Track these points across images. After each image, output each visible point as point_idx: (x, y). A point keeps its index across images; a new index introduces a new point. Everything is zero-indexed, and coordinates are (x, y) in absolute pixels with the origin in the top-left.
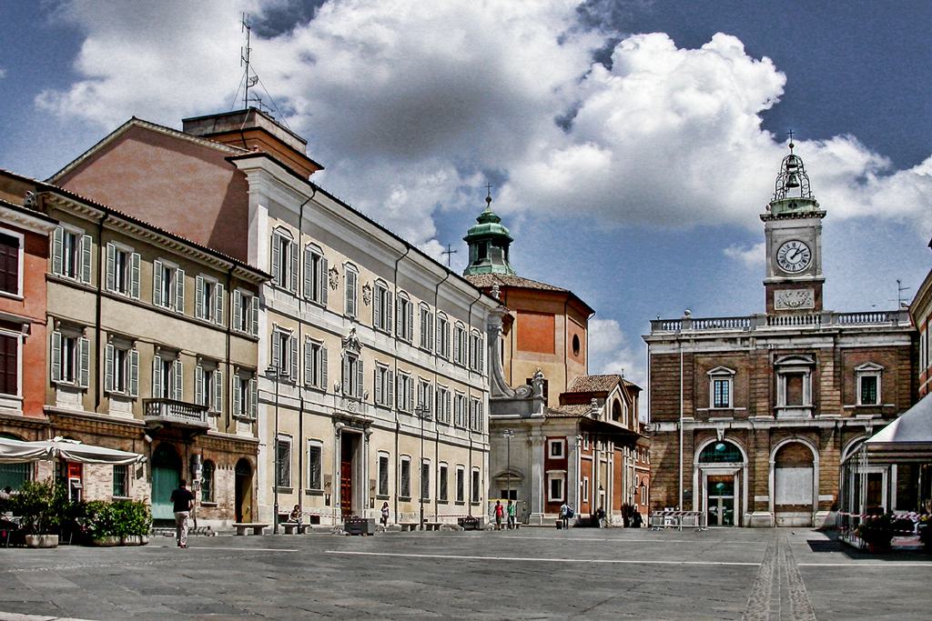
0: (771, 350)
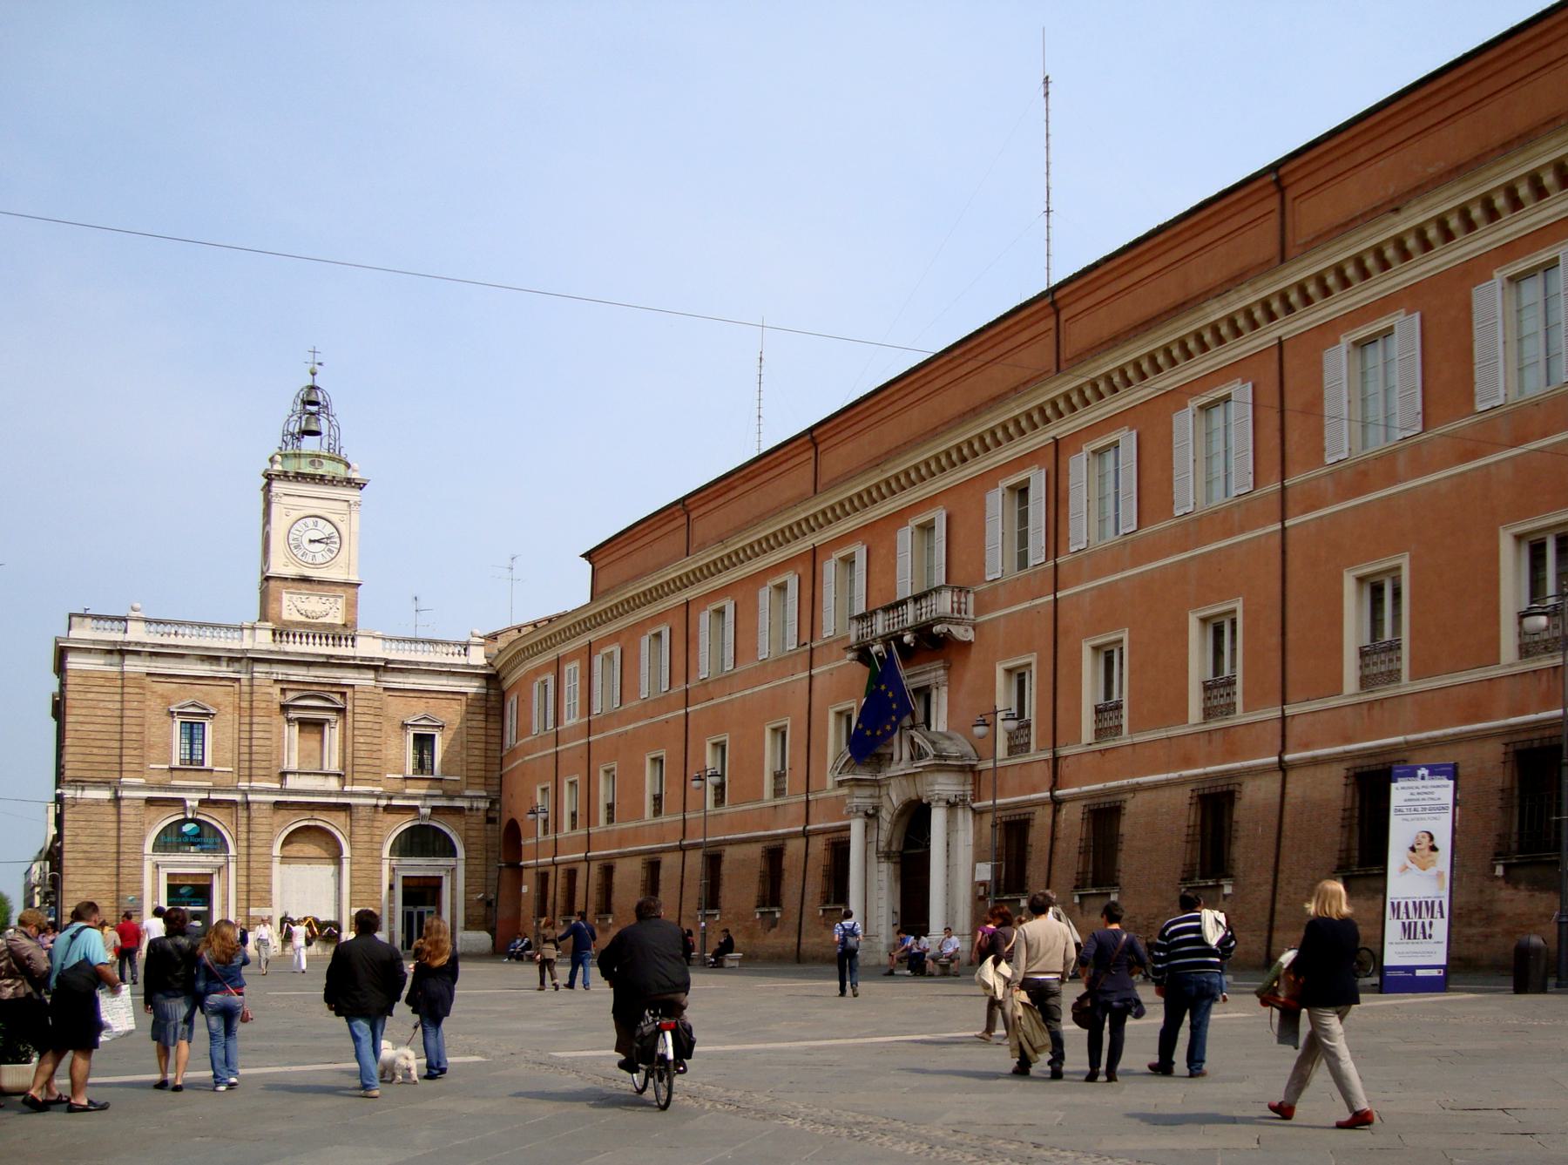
0: (276, 681)
